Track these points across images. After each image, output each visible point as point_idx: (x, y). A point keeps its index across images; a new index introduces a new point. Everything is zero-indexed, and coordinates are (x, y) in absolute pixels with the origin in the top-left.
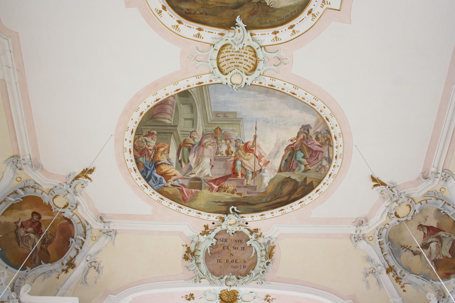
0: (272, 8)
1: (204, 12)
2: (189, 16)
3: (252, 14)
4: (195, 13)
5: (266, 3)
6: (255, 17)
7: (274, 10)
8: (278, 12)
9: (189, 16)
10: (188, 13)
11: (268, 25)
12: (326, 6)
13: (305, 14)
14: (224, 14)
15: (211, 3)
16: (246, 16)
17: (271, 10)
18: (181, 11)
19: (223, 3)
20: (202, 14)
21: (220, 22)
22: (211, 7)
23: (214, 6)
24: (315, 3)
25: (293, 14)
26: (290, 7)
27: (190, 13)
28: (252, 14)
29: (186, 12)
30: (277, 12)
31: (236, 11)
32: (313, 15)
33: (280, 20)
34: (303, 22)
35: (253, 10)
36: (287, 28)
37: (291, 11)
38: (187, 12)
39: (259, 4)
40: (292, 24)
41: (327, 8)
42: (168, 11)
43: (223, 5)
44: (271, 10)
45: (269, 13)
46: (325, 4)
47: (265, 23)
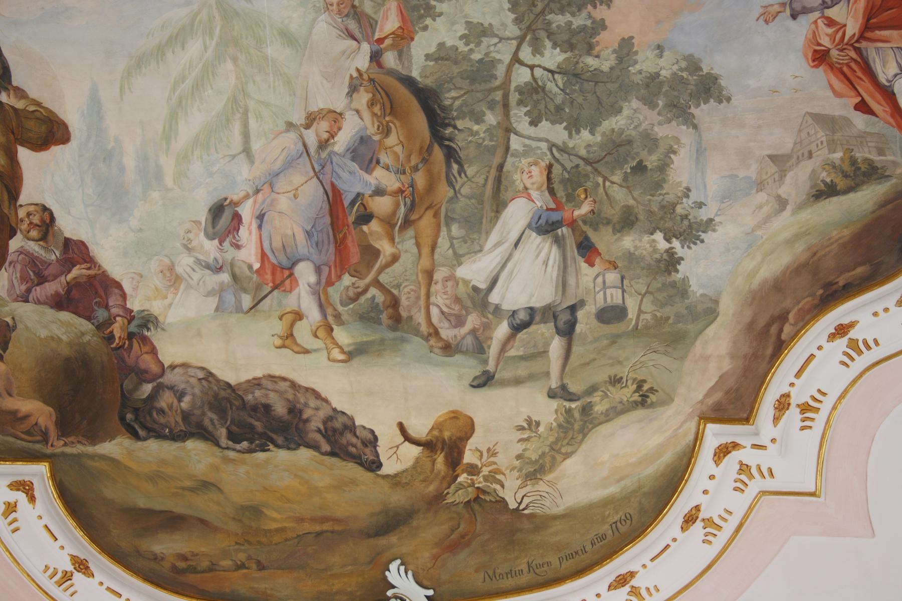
0: (532, 516)
1: (250, 558)
2: (191, 578)
3: (452, 545)
4: (213, 568)
5: (503, 501)
6: (463, 555)
7: (541, 522)
8: (557, 526)
9: (191, 578)
10: (183, 571)
11: (524, 579)
12: (756, 485)
13: (670, 522)
14: (335, 559)
15: (273, 526)
16: (425, 556)
17: (526, 525)
18: (153, 565)
19: (324, 520)
20: (242, 566)
21: (323, 588)
22: (276, 539)
23: (290, 535)
24: (710, 485)
25: (623, 529)
26: (606, 503)
27: (193, 570)
28: (452, 545)
29: (174, 568)
30: (554, 529)
31: (382, 541)
32: (709, 522)
33: (571, 556)
34: (665, 558)
35: (453, 531)
36: (602, 588)
37: (611, 520)
38: (182, 565)
39: (476, 507)
40: (623, 571)
41: (764, 493)
42: (98, 577)
43: (325, 527)
44: (526, 525)
45: (519, 536)
46: (751, 477)
47: (510, 573)
